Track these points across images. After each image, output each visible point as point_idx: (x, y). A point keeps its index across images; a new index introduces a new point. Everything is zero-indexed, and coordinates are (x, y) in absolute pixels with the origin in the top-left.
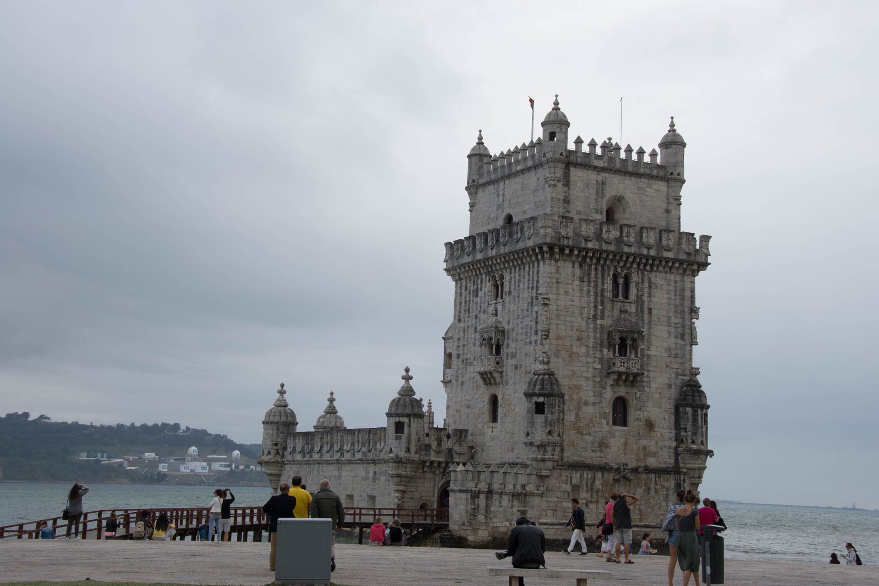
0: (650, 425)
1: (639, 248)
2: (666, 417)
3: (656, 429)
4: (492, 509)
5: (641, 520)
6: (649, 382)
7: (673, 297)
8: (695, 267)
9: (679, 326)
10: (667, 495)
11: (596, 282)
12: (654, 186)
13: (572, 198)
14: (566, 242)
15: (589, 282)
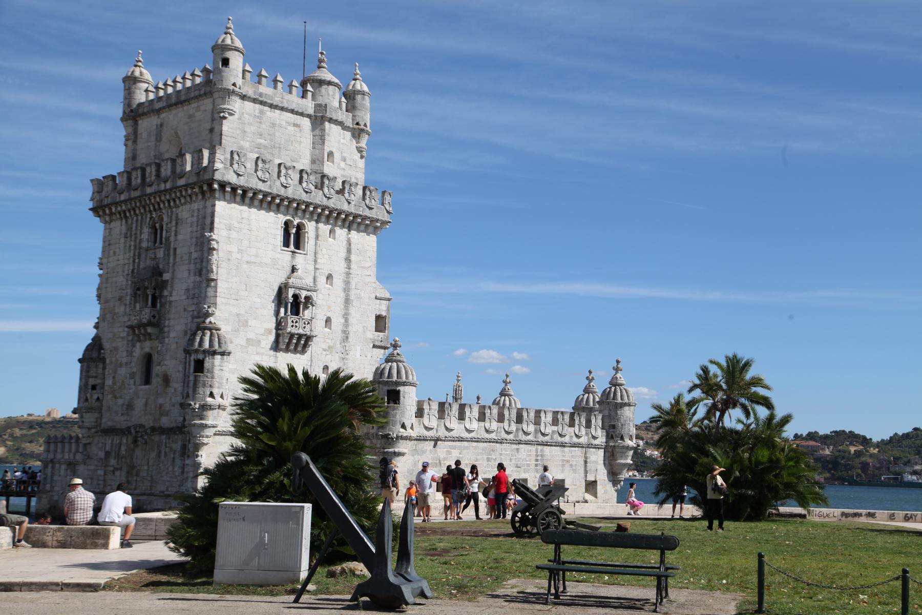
0: (166, 380)
1: (158, 185)
2: (181, 369)
3: (171, 384)
4: (55, 478)
5: (151, 486)
6: (169, 332)
7: (195, 229)
8: (205, 188)
9: (198, 261)
10: (174, 458)
11: (136, 234)
12: (202, 108)
13: (138, 152)
14: (105, 202)
15: (131, 236)
